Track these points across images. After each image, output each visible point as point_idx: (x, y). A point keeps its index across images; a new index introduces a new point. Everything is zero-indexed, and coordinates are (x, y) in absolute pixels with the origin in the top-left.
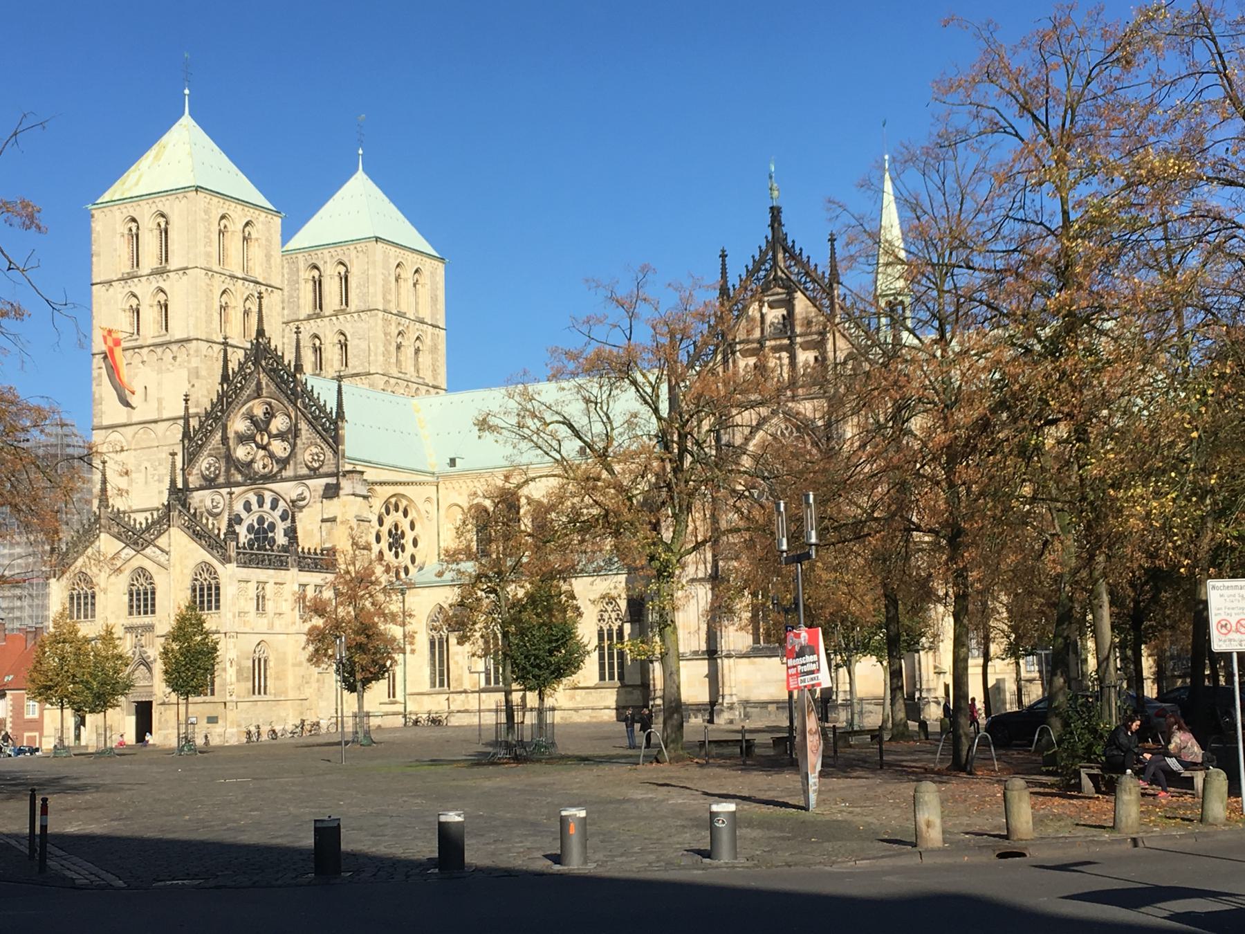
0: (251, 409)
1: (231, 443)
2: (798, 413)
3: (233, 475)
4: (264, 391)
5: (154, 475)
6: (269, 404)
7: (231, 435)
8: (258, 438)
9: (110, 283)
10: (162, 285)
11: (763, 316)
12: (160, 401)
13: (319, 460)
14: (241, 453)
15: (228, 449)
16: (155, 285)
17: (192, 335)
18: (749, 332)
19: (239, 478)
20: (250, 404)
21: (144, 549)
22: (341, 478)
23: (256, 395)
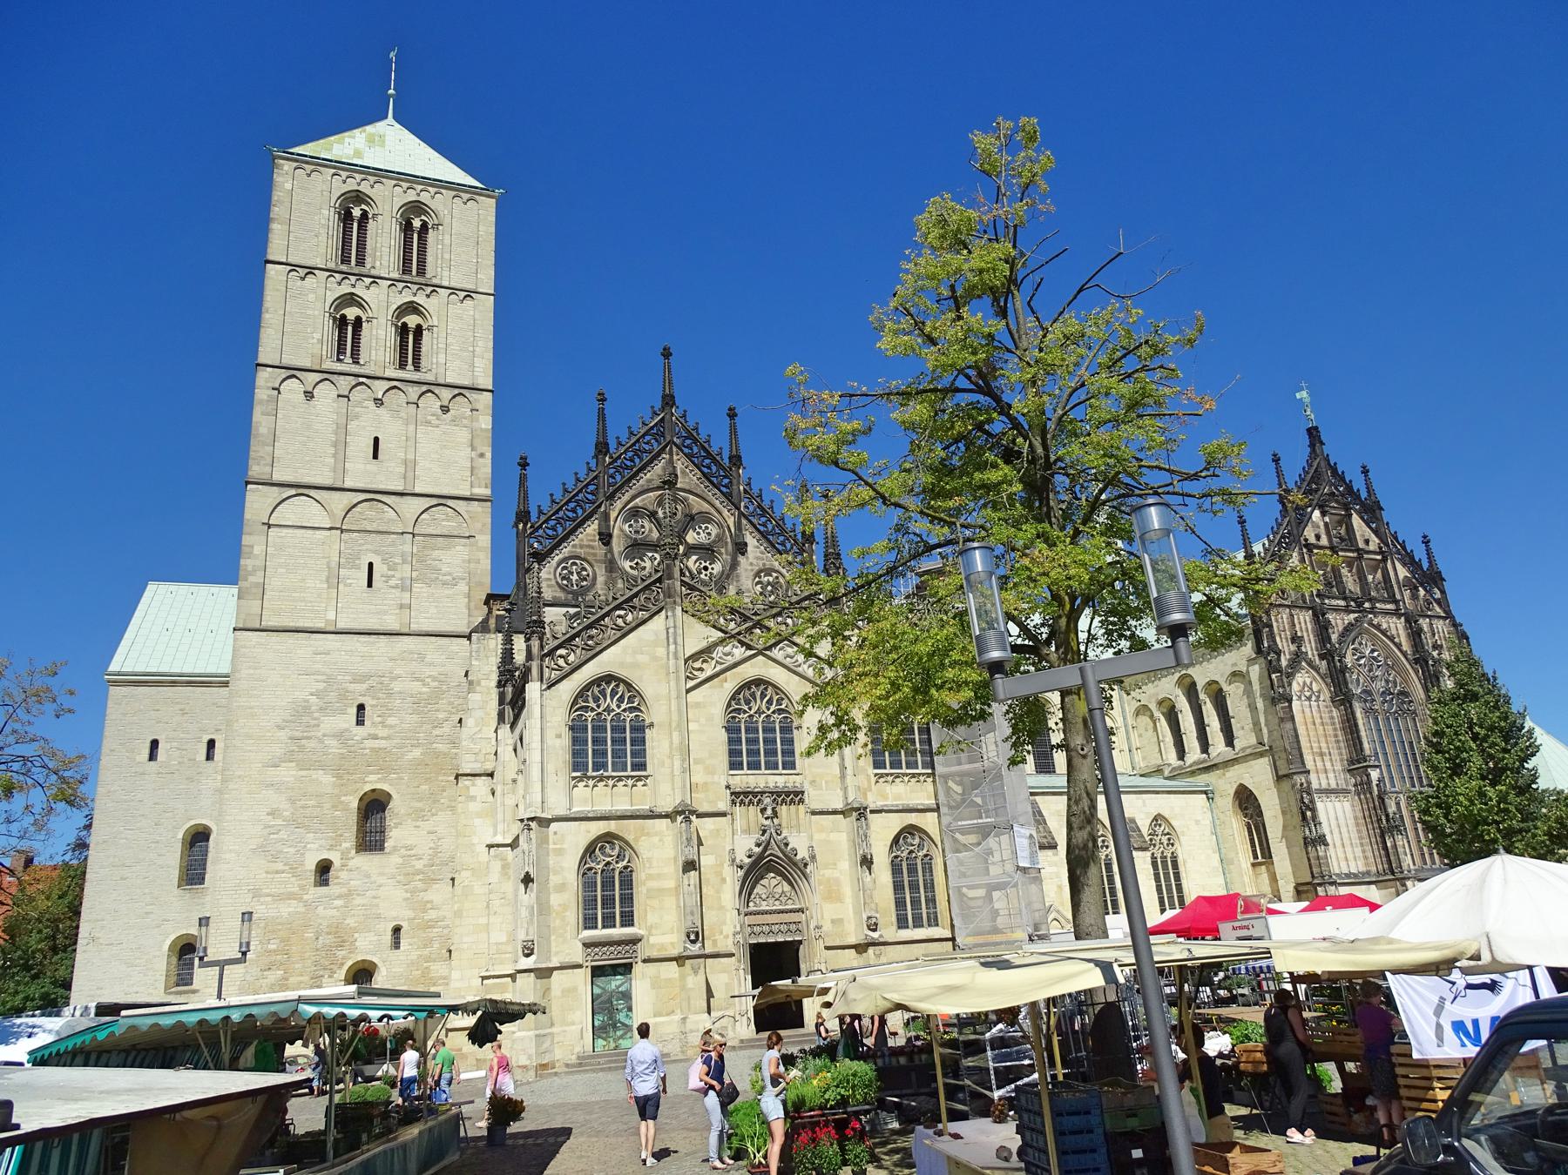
2: (1378, 627)
5: (389, 577)
6: (686, 499)
7: (615, 531)
9: (311, 270)
10: (420, 299)
11: (1326, 524)
12: (410, 466)
15: (611, 551)
18: (1318, 537)
21: (769, 648)
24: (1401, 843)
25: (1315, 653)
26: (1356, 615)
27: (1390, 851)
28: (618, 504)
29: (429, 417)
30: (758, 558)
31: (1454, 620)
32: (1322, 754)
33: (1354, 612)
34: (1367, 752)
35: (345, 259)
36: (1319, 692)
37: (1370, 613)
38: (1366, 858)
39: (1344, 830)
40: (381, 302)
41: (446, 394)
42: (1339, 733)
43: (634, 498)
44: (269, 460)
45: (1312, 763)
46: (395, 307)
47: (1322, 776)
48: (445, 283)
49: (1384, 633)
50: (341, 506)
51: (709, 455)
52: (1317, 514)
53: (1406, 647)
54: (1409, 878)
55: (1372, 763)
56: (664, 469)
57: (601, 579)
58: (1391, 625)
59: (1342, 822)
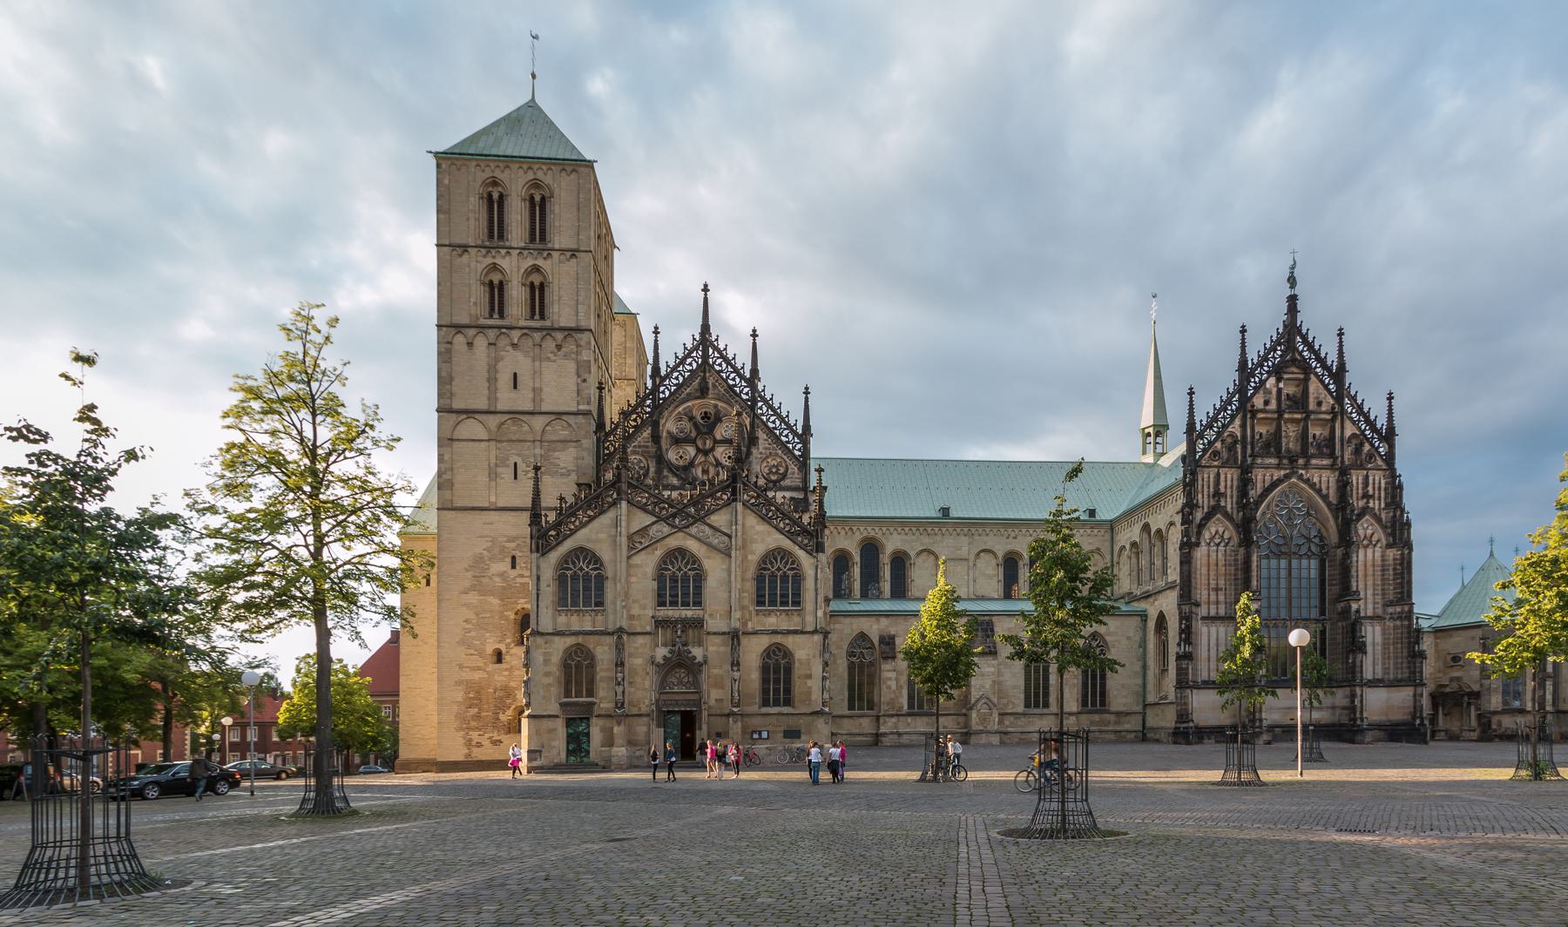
0: (690, 409)
1: (664, 443)
2: (1307, 481)
3: (666, 477)
4: (711, 391)
6: (716, 406)
8: (700, 443)
10: (540, 262)
11: (1279, 391)
12: (537, 391)
13: (776, 473)
14: (672, 456)
15: (660, 448)
16: (530, 262)
17: (583, 324)
18: (1266, 403)
19: (675, 481)
20: (689, 404)
22: (809, 494)
23: (698, 394)
28: (666, 414)
29: (550, 355)
30: (766, 448)
35: (491, 236)
40: (513, 266)
41: (559, 336)
43: (677, 407)
44: (449, 395)
46: (523, 270)
48: (557, 247)
49: (1312, 486)
50: (495, 424)
51: (736, 370)
52: (1272, 380)
56: (700, 384)
57: (652, 470)
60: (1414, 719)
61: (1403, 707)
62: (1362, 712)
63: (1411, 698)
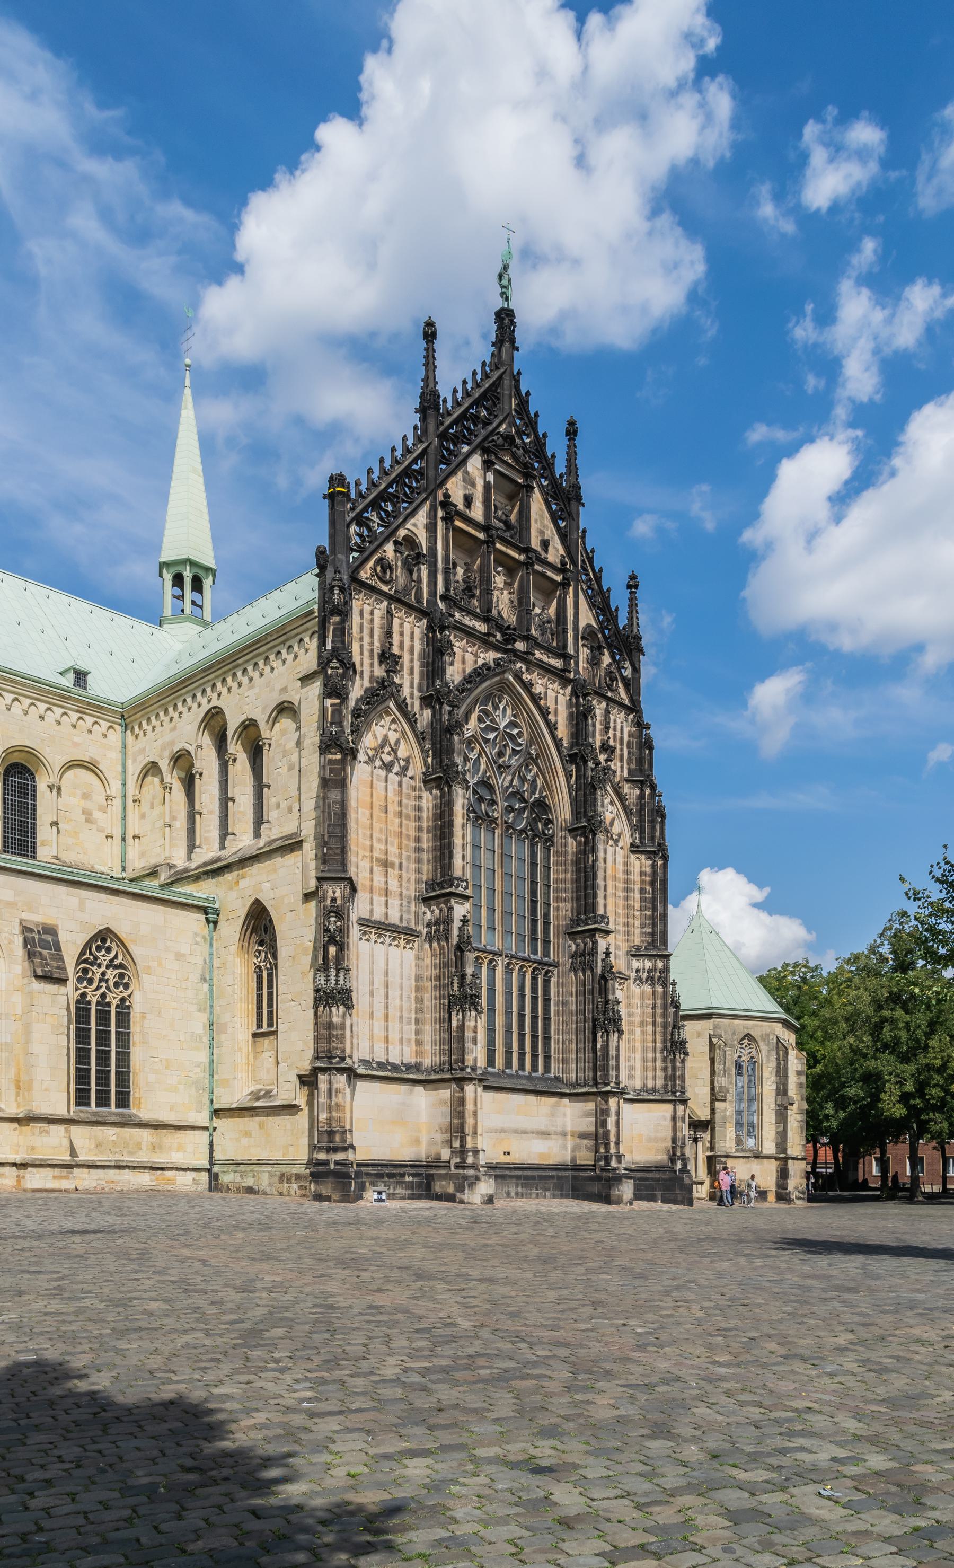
2: (528, 686)
24: (472, 1023)
25: (417, 694)
26: (499, 655)
27: (454, 1034)
31: (640, 717)
32: (386, 864)
33: (496, 648)
34: (458, 873)
36: (407, 760)
37: (523, 660)
38: (419, 1043)
39: (394, 993)
42: (424, 836)
45: (367, 875)
47: (379, 900)
49: (535, 699)
53: (563, 731)
54: (471, 1080)
55: (460, 890)
58: (550, 693)
59: (394, 979)
60: (673, 1160)
61: (656, 1140)
62: (617, 1143)
63: (668, 1123)
